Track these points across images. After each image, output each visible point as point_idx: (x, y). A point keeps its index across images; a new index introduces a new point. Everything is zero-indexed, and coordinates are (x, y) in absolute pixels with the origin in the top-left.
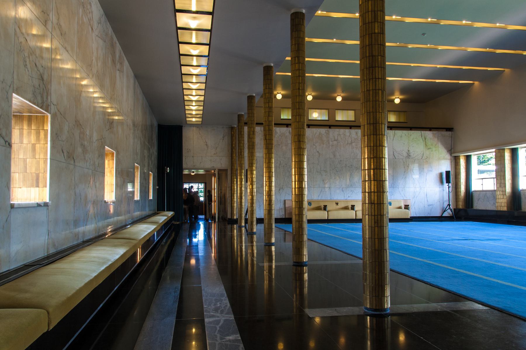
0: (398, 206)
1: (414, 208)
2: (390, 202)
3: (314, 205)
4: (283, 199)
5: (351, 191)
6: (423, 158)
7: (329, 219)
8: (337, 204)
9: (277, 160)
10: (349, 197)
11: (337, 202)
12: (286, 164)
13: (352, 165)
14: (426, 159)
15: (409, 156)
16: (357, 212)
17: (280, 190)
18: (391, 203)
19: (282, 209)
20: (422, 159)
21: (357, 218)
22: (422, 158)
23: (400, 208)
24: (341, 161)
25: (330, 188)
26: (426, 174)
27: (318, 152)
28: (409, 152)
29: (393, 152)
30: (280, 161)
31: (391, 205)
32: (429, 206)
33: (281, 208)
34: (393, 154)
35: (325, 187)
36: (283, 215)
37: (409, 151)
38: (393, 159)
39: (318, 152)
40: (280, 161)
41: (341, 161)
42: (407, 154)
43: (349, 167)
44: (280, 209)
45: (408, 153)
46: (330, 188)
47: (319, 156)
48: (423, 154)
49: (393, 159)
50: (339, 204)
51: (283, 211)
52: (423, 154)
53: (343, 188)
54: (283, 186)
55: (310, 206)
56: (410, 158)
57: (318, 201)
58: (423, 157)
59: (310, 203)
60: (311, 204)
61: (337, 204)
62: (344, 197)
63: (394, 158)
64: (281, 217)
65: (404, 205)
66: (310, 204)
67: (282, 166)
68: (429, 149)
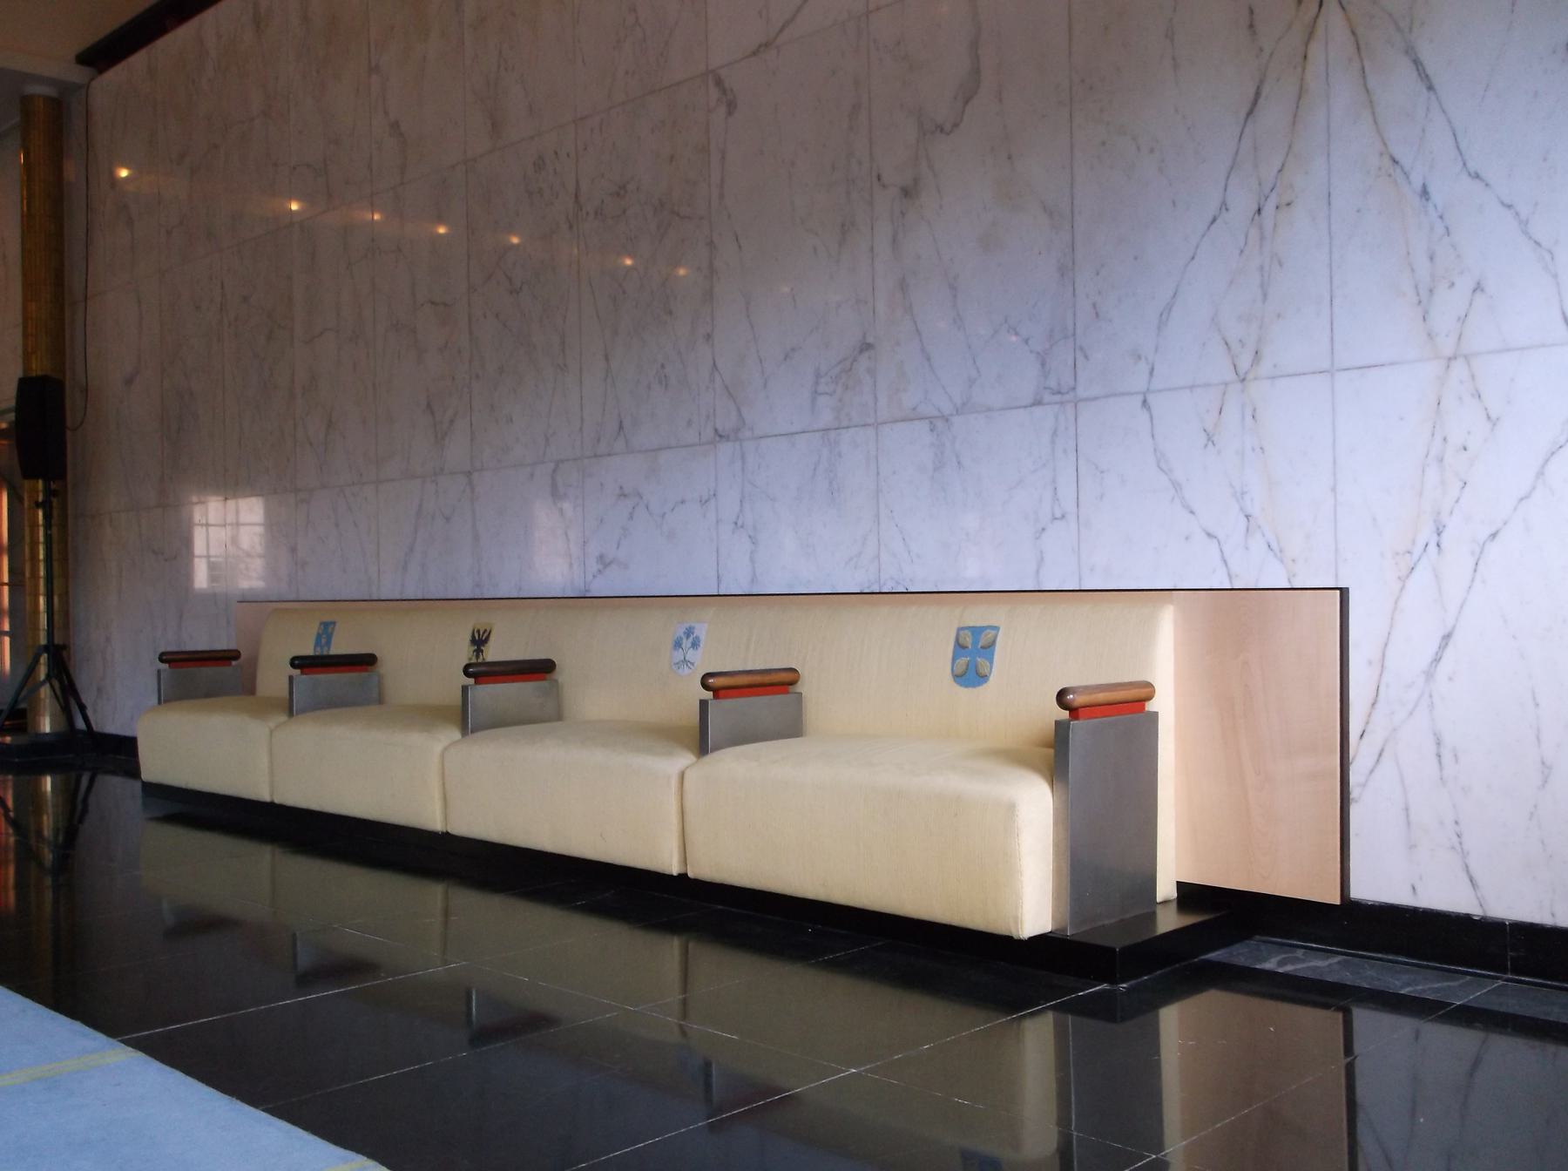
10: (604, 562)
18: (991, 645)
31: (981, 678)
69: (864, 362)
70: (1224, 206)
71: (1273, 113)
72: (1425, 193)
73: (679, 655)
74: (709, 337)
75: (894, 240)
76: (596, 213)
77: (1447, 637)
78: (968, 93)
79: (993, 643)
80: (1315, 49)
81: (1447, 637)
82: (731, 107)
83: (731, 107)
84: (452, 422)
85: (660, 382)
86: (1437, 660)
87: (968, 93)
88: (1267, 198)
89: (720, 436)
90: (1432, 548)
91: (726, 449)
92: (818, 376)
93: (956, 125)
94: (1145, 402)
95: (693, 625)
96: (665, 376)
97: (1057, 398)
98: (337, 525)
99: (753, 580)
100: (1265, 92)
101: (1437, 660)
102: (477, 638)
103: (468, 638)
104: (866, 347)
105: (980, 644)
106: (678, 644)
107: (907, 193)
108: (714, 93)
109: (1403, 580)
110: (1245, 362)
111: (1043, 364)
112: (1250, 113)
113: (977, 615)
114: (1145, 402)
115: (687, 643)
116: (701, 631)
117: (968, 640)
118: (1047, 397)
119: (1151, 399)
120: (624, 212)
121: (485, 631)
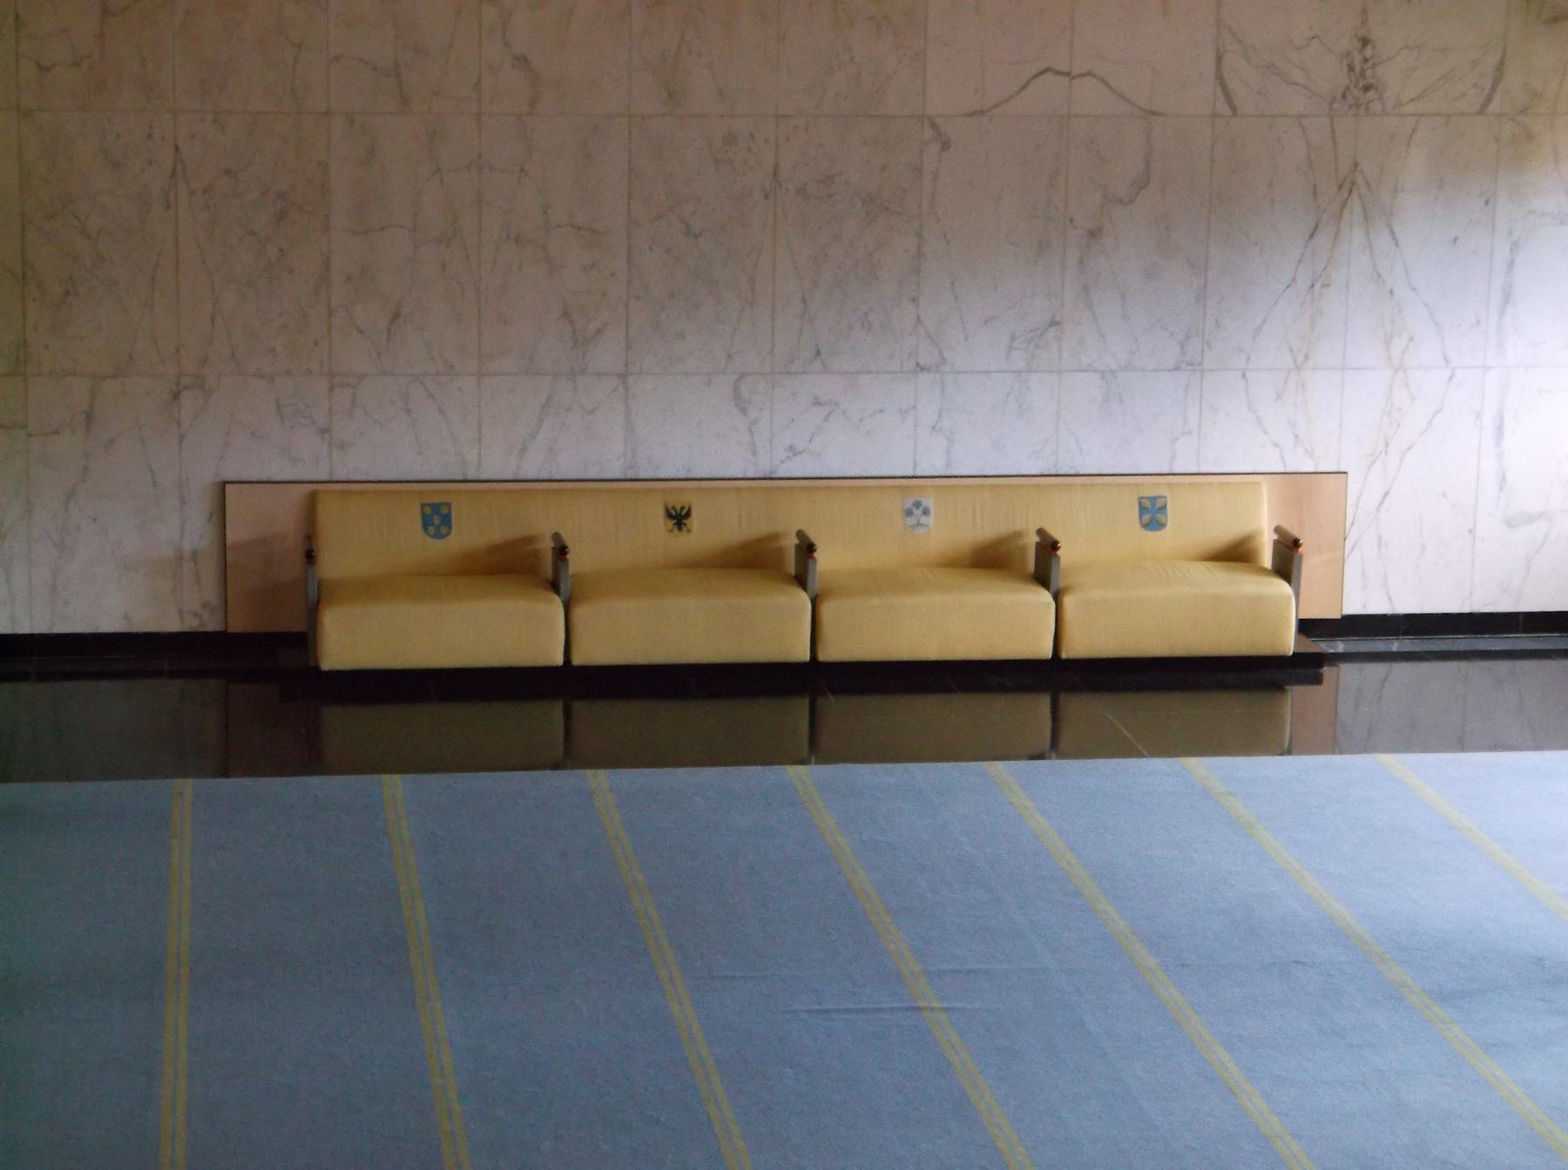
0: (1223, 532)
1: (1380, 538)
2: (1154, 499)
3: (471, 532)
4: (204, 474)
5: (817, 402)
6: (1494, 107)
7: (577, 660)
8: (679, 518)
9: (150, 137)
10: (793, 451)
11: (677, 502)
12: (228, 172)
13: (828, 180)
14: (1525, 110)
15: (1367, 88)
16: (827, 610)
17: (176, 396)
18: (1164, 507)
19: (195, 555)
20: (1482, 111)
21: (822, 657)
22: (1489, 100)
23: (1236, 554)
24: (730, 139)
25: (623, 377)
26: (1515, 246)
27: (522, 61)
28: (1368, 52)
29: (1219, 59)
30: (177, 149)
32: (1511, 523)
33: (187, 546)
34: (1220, 78)
35: (583, 372)
36: (205, 605)
37: (1365, 42)
38: (1215, 115)
39: (522, 61)
40: (177, 149)
41: (730, 139)
42: (1351, 68)
43: (801, 191)
44: (180, 558)
45: (1357, 59)
46: (623, 377)
47: (533, 102)
48: (1500, 69)
49: (1215, 115)
50: (694, 522)
51: (210, 572)
52: (1500, 69)
53: (742, 376)
54: (204, 361)
55: (438, 535)
56: (1376, 107)
57: (520, 487)
58: (1493, 90)
59: (436, 507)
60: (447, 520)
61: (679, 518)
62: (755, 453)
63: (1223, 107)
64: (190, 624)
65: (1278, 530)
66: (437, 520)
67: (192, 193)
68: (1555, 20)
69: (1052, 332)
70: (1294, 280)
71: (1323, 239)
72: (1391, 292)
73: (911, 521)
74: (914, 300)
75: (1081, 262)
76: (798, 192)
77: (1386, 494)
78: (1142, 183)
79: (1165, 506)
80: (1346, 213)
81: (1386, 494)
82: (945, 146)
83: (945, 146)
84: (599, 331)
85: (863, 326)
86: (1382, 503)
87: (1142, 183)
88: (1317, 280)
89: (920, 368)
90: (1383, 454)
91: (925, 378)
92: (1013, 339)
93: (1131, 201)
94: (1244, 375)
95: (919, 499)
96: (868, 321)
97: (1190, 367)
98: (408, 411)
99: (948, 466)
100: (1320, 226)
101: (1382, 503)
102: (674, 513)
103: (661, 512)
104: (1054, 323)
105: (1157, 507)
106: (909, 513)
107: (1094, 234)
108: (928, 133)
109: (1369, 468)
110: (1300, 360)
111: (1182, 348)
112: (1312, 236)
113: (1150, 489)
114: (1244, 375)
115: (918, 512)
116: (928, 502)
117: (1147, 504)
118: (1184, 366)
119: (1248, 374)
120: (830, 196)
121: (682, 508)
